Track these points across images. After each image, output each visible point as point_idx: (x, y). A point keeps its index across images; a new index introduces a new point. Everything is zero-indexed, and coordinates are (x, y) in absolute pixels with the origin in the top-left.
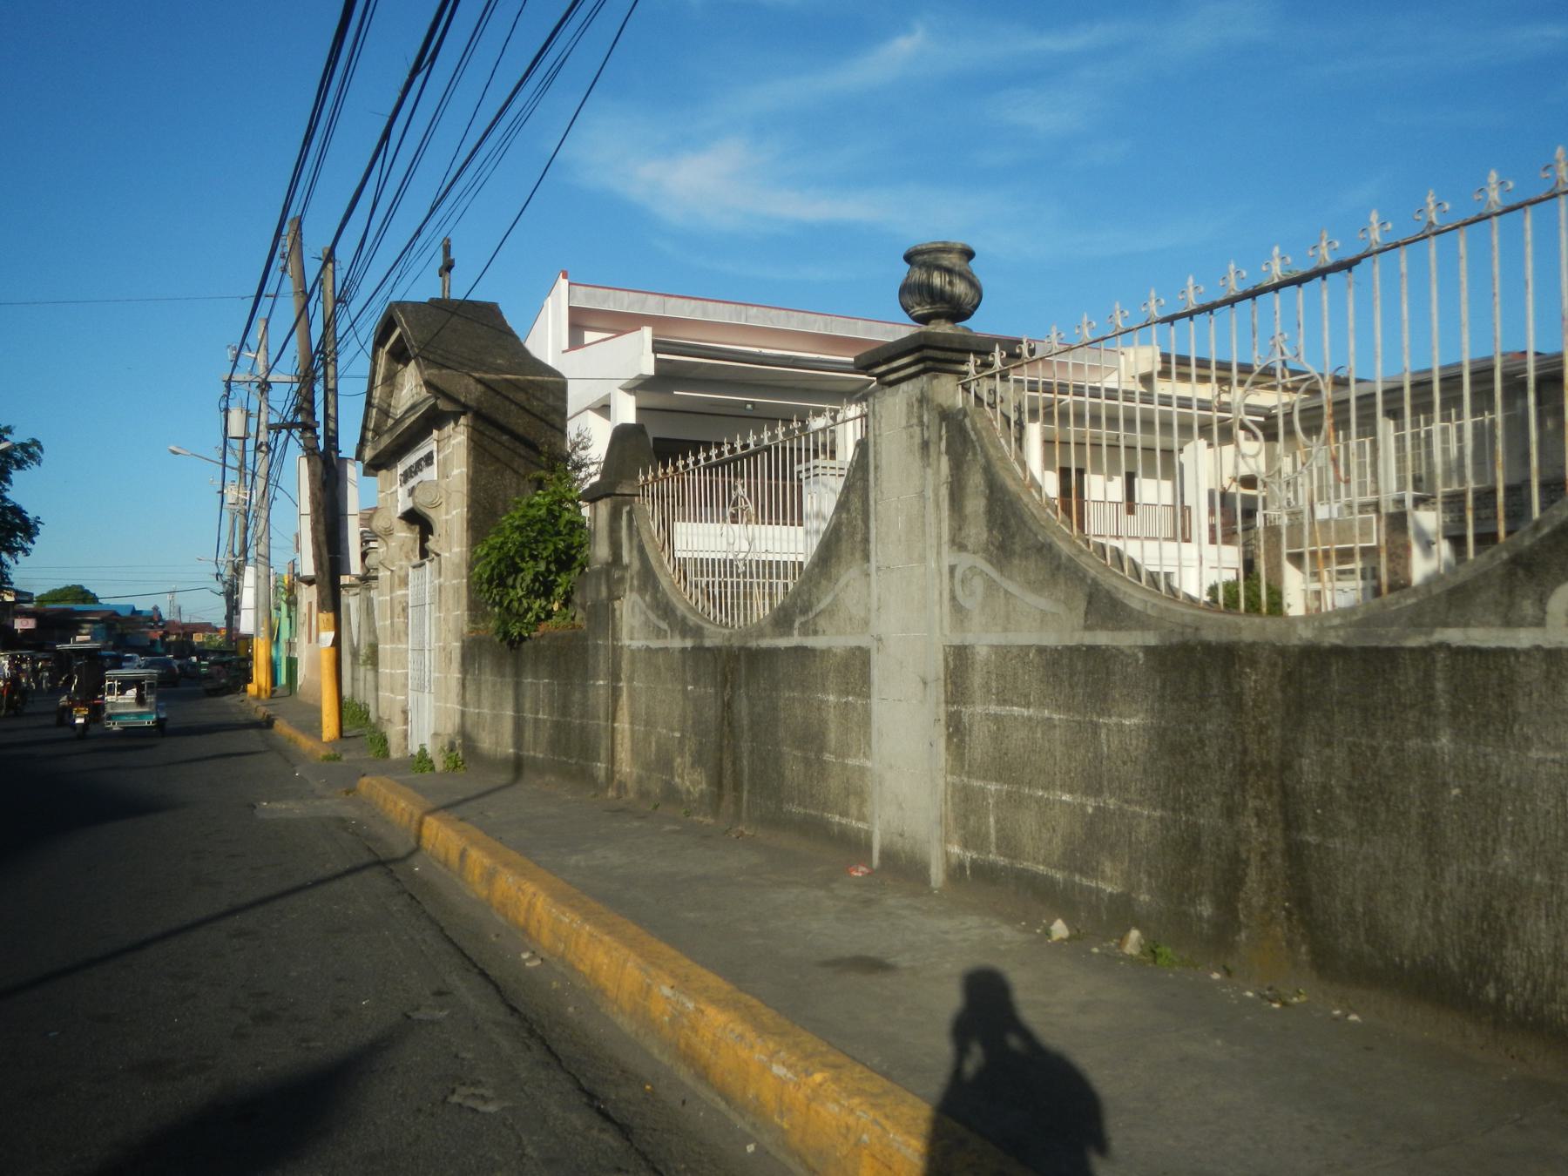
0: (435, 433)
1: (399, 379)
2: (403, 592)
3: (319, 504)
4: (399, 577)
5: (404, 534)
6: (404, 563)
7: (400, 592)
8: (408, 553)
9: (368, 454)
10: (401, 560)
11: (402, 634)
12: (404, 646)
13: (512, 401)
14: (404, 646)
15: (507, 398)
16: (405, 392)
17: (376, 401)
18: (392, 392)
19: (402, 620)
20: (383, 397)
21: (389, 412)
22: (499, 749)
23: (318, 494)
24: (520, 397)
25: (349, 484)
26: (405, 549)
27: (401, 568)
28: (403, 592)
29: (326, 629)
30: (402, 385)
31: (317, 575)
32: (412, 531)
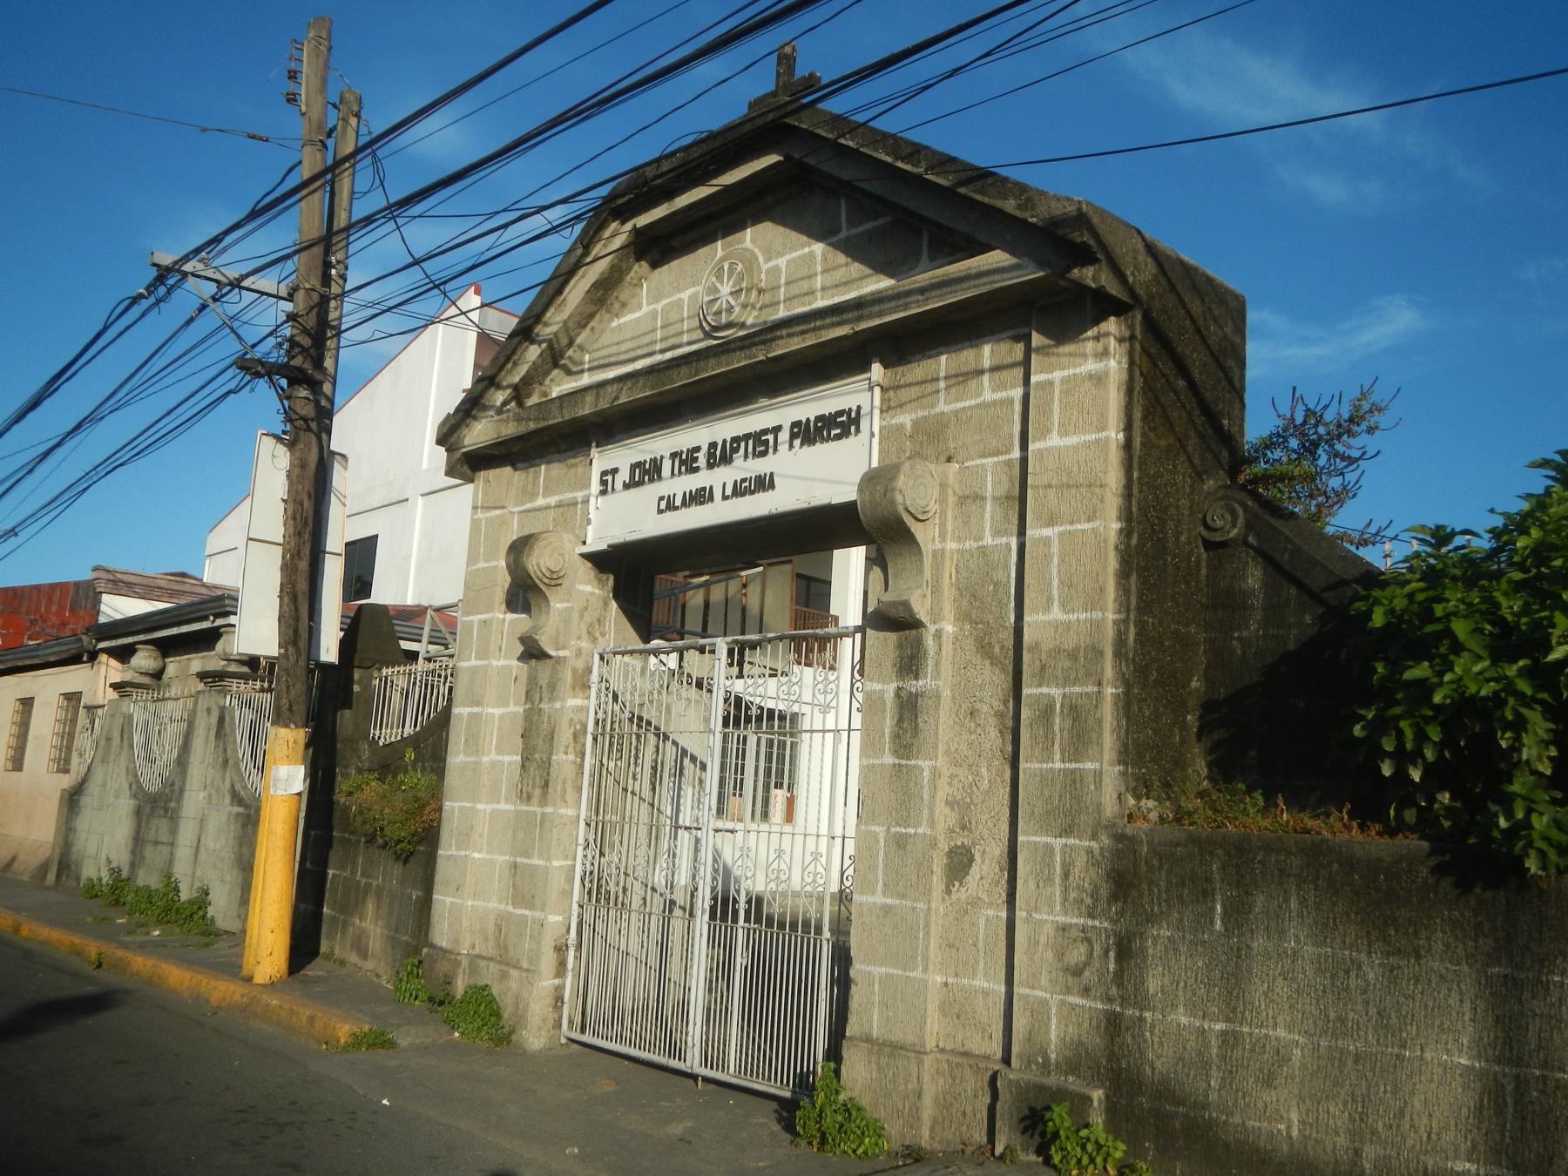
0: (877, 370)
1: (624, 293)
2: (579, 702)
3: (306, 524)
4: (574, 671)
5: (588, 588)
6: (584, 644)
7: (572, 702)
8: (591, 625)
9: (479, 434)
10: (579, 638)
11: (570, 790)
12: (571, 812)
13: (1184, 306)
14: (571, 812)
15: (1181, 301)
16: (628, 318)
17: (546, 331)
18: (591, 316)
19: (571, 757)
20: (571, 324)
21: (562, 356)
22: (1370, 1152)
23: (306, 504)
24: (1196, 307)
25: (333, 497)
26: (588, 618)
27: (579, 653)
28: (579, 702)
29: (289, 760)
30: (624, 305)
31: (285, 656)
32: (601, 583)
